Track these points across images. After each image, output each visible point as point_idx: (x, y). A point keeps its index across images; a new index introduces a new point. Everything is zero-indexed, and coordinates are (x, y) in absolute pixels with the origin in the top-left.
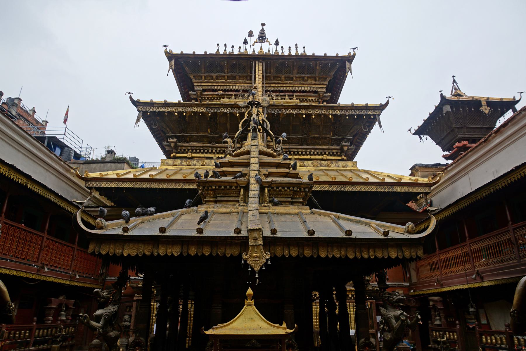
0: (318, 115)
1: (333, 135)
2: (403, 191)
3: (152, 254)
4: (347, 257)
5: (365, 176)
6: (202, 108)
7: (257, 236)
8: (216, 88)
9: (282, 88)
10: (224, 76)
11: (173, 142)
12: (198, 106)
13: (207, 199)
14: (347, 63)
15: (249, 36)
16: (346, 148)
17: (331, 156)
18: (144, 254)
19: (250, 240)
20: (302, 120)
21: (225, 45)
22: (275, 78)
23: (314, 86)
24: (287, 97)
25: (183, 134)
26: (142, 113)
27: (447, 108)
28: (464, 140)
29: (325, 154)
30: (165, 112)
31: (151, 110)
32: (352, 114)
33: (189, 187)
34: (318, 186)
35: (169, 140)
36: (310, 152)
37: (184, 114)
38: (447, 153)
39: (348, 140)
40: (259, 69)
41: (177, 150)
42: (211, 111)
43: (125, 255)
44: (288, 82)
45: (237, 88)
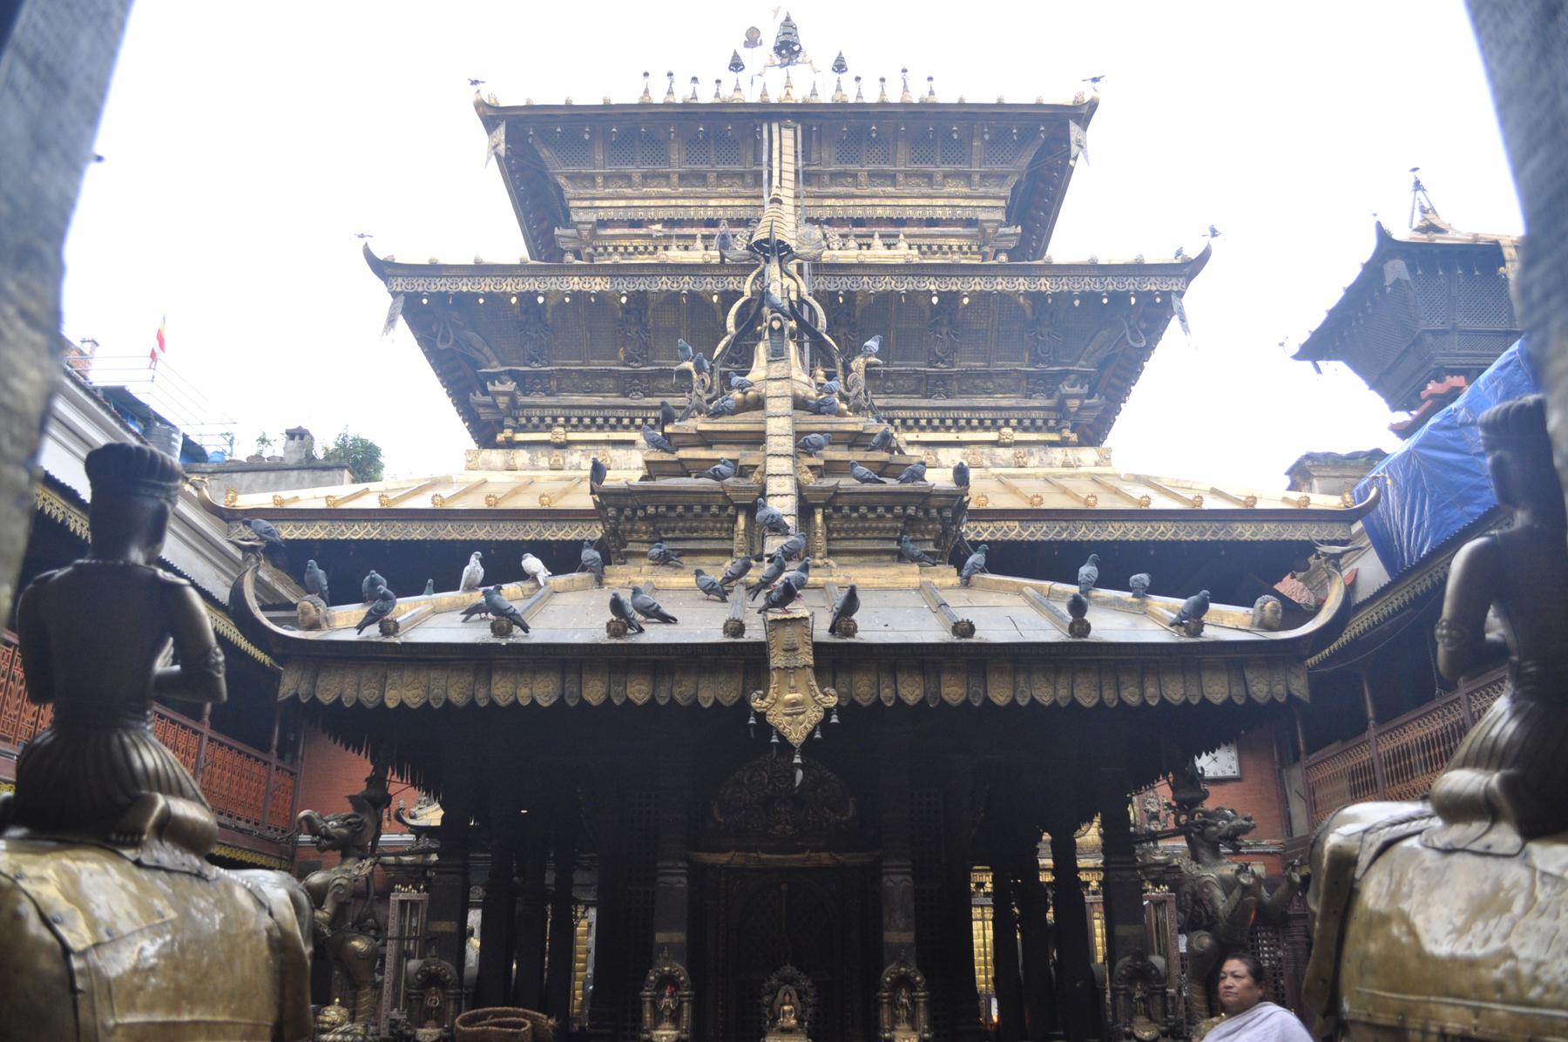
0: (981, 297)
1: (1033, 363)
2: (1260, 537)
3: (472, 702)
4: (1074, 702)
5: (1138, 492)
6: (598, 280)
7: (797, 640)
8: (641, 214)
9: (859, 213)
12: (582, 272)
13: (631, 547)
14: (1074, 128)
15: (747, 45)
16: (1077, 402)
17: (1026, 430)
18: (447, 701)
19: (773, 652)
20: (928, 314)
21: (670, 74)
22: (836, 177)
24: (877, 242)
25: (536, 367)
26: (402, 298)
27: (1397, 269)
28: (1453, 373)
29: (1007, 423)
30: (477, 296)
31: (433, 289)
32: (1092, 292)
33: (560, 536)
34: (985, 525)
35: (490, 388)
36: (956, 421)
37: (541, 300)
38: (1403, 417)
39: (1082, 377)
40: (784, 150)
41: (516, 419)
42: (626, 286)
43: (391, 704)
44: (879, 190)
45: (710, 213)
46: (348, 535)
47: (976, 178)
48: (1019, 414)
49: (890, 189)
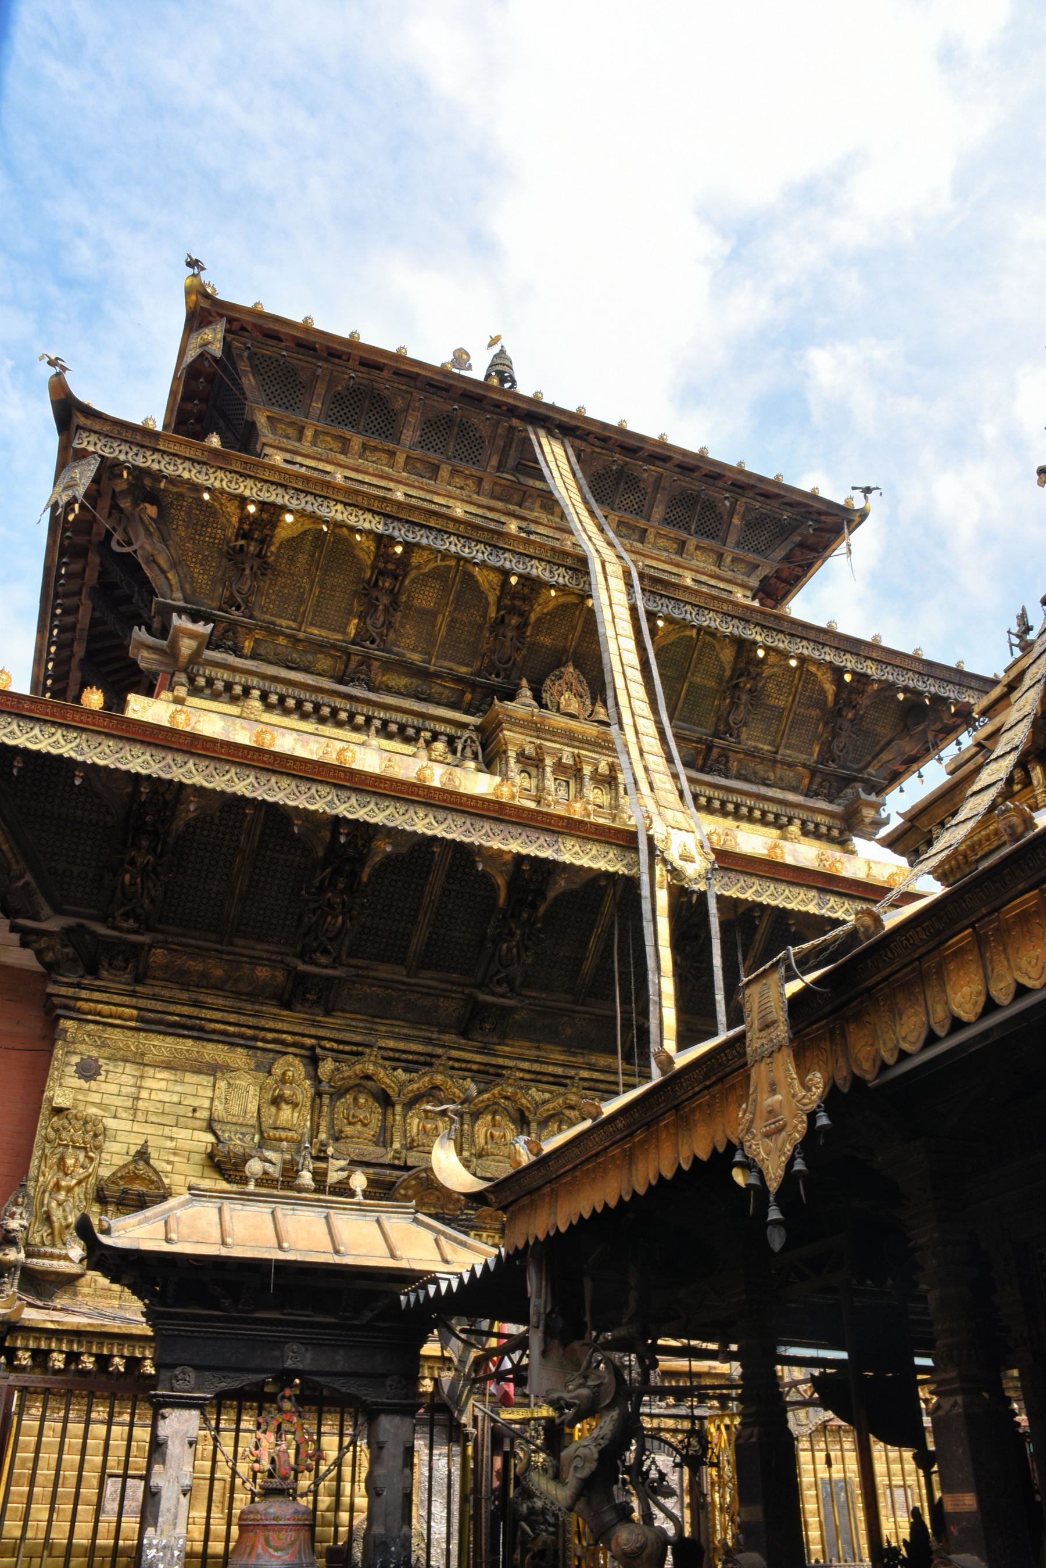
10: (392, 454)
11: (192, 635)
12: (353, 499)
23: (713, 582)
25: (235, 615)
31: (140, 462)
36: (737, 806)
46: (21, 741)
47: (728, 560)
48: (804, 815)
49: (640, 545)
